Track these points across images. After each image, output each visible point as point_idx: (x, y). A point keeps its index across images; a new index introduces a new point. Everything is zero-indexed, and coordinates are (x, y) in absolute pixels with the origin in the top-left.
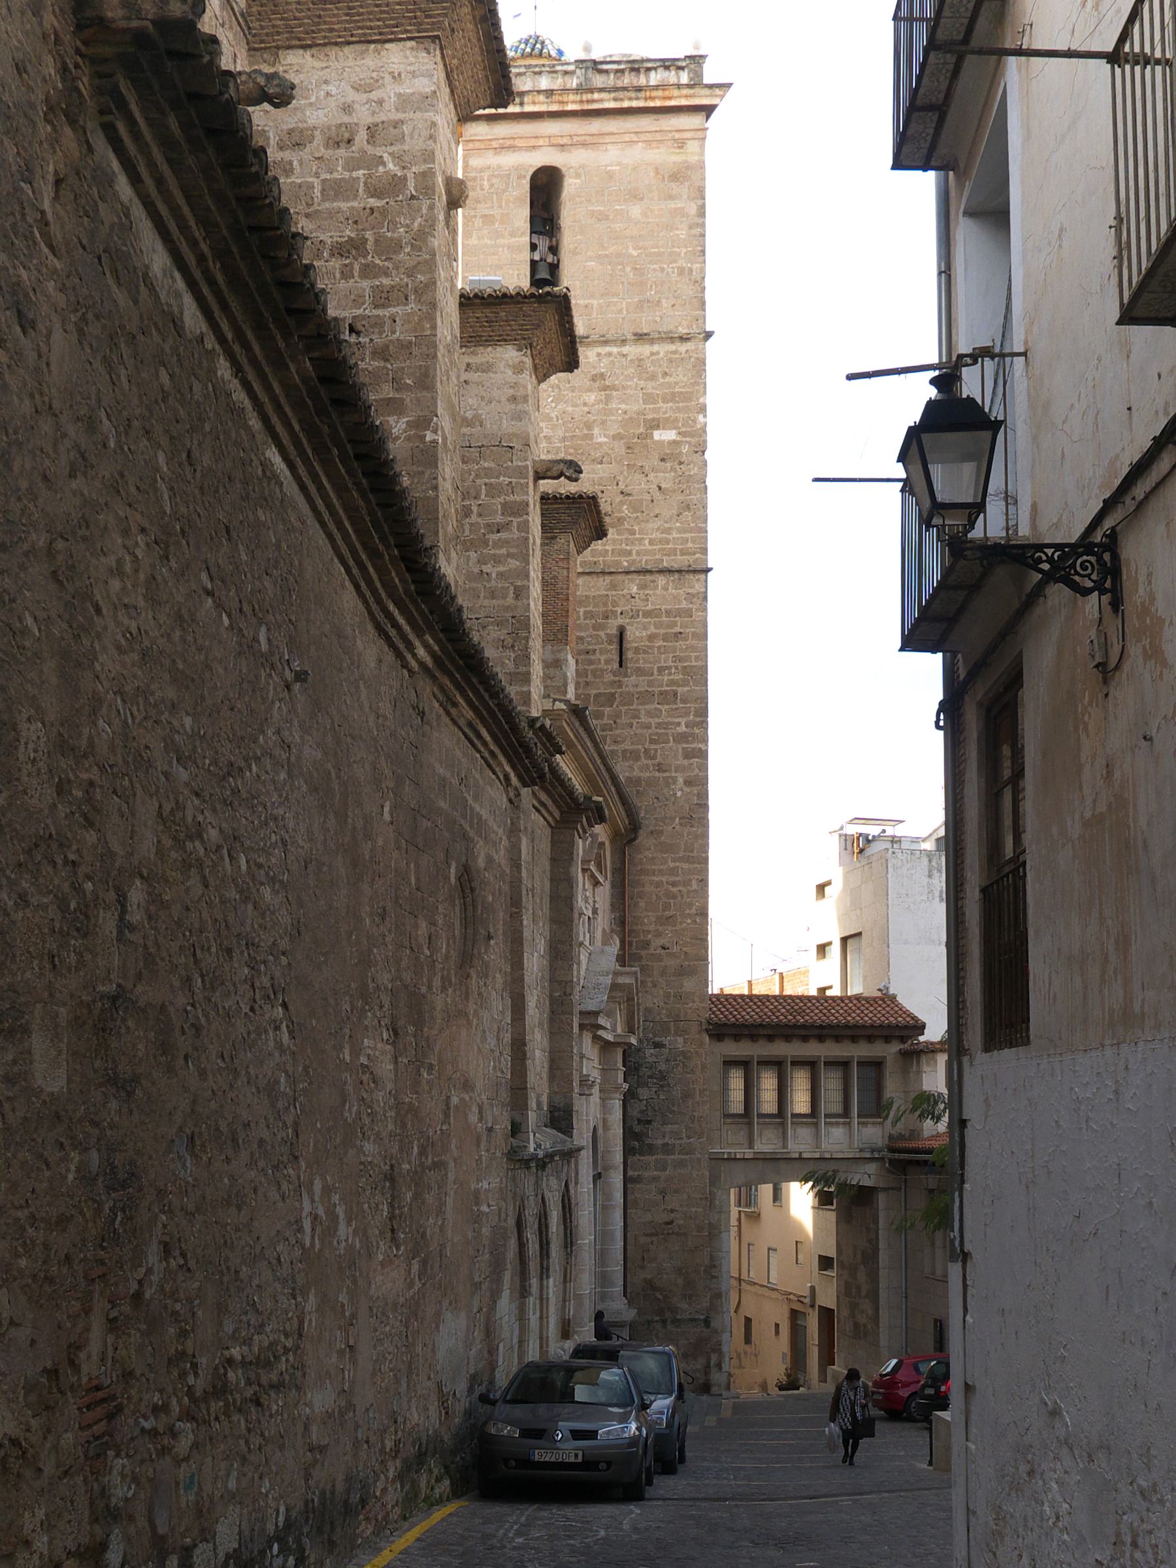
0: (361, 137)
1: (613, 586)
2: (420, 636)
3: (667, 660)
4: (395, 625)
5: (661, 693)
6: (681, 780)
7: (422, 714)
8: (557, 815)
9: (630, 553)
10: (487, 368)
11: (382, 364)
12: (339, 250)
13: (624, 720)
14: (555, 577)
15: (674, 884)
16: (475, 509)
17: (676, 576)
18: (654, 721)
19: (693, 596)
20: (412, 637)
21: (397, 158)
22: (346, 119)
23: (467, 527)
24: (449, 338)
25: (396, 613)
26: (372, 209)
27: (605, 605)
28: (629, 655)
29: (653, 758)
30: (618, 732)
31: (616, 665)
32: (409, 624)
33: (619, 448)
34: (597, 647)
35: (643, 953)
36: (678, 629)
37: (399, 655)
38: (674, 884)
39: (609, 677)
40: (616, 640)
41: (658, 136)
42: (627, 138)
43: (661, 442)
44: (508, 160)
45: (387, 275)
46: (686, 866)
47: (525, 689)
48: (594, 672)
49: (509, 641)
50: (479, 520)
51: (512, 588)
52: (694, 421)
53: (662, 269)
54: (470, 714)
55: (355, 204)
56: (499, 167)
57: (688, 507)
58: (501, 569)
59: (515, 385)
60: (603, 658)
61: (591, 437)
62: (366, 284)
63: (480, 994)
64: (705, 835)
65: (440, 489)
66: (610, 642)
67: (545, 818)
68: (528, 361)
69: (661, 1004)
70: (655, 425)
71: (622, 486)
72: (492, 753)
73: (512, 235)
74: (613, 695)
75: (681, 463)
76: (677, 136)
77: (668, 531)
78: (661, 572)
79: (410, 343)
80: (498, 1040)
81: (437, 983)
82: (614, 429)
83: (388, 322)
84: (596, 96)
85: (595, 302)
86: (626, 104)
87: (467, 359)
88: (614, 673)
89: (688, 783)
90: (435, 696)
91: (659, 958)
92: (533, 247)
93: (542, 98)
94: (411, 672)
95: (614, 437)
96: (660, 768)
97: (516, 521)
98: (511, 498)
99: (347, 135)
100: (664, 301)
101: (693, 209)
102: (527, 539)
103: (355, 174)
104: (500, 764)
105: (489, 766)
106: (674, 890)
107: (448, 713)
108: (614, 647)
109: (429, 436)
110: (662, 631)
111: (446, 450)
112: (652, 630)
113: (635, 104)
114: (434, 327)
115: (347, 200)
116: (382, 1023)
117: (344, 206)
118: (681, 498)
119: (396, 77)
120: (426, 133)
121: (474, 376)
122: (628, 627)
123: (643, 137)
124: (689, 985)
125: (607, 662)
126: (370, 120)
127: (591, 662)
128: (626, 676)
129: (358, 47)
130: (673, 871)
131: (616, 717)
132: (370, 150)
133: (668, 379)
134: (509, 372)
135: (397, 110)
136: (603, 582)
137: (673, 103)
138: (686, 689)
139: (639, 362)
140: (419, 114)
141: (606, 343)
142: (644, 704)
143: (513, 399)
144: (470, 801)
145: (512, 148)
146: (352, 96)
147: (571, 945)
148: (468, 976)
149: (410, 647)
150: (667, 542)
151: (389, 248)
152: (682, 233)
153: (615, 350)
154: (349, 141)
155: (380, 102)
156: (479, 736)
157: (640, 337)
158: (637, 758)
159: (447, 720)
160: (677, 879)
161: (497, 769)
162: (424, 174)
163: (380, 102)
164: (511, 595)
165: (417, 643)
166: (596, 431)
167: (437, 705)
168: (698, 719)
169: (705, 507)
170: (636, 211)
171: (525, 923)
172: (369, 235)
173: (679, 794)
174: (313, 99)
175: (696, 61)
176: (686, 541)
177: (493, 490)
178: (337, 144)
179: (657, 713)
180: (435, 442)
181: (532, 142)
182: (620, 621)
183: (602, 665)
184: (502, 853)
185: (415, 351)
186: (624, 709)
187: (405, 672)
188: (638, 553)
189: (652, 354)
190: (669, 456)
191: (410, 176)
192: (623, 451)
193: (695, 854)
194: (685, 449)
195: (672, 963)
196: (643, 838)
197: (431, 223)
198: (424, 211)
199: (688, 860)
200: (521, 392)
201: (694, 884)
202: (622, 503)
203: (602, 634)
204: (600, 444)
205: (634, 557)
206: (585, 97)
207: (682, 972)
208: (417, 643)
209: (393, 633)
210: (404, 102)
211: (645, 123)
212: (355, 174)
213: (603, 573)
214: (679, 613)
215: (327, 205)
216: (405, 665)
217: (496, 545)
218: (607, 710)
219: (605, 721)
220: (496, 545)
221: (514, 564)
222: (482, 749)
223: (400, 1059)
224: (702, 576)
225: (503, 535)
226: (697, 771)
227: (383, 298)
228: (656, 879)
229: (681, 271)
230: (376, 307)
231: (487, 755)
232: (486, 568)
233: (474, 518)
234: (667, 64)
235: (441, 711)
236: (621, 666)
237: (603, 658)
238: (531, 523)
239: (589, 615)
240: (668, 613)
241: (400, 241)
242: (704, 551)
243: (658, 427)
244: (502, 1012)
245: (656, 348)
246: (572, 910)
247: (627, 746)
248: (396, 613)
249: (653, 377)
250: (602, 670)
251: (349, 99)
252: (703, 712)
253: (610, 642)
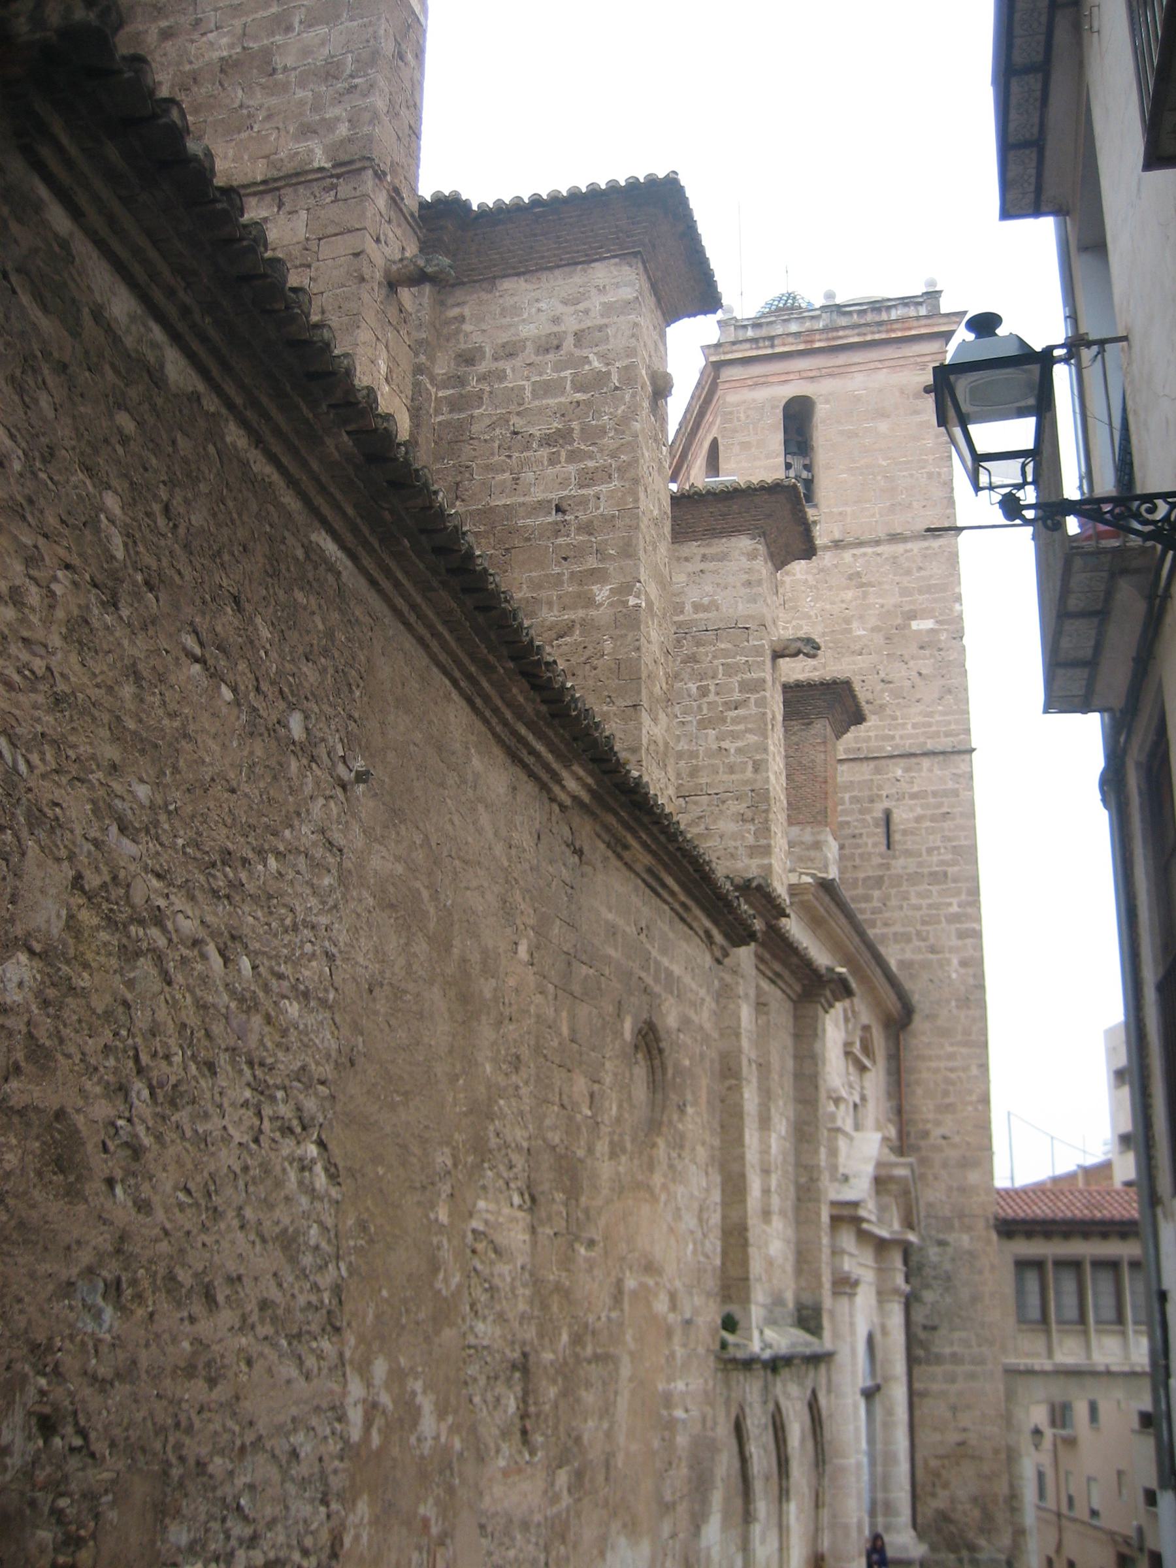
0: (569, 342)
1: (878, 771)
2: (567, 767)
3: (935, 840)
4: (532, 752)
5: (931, 874)
6: (955, 962)
7: (579, 852)
8: (798, 988)
9: (893, 738)
10: (723, 557)
11: (586, 538)
12: (548, 441)
13: (893, 902)
14: (813, 761)
15: (952, 1070)
16: (712, 688)
17: (941, 758)
18: (924, 902)
19: (959, 776)
20: (556, 766)
21: (602, 356)
22: (556, 329)
23: (705, 707)
24: (656, 512)
25: (531, 738)
26: (578, 403)
27: (870, 789)
28: (897, 837)
29: (924, 940)
30: (887, 915)
31: (883, 848)
32: (551, 751)
33: (879, 639)
34: (864, 831)
35: (922, 1143)
36: (945, 810)
37: (544, 787)
38: (952, 1070)
39: (877, 860)
40: (883, 823)
41: (901, 362)
42: (872, 366)
43: (919, 631)
44: (762, 394)
45: (591, 458)
46: (964, 1050)
47: (766, 862)
48: (861, 856)
49: (749, 814)
50: (716, 698)
51: (750, 763)
52: (951, 610)
53: (911, 476)
54: (648, 859)
55: (563, 399)
56: (754, 400)
57: (949, 691)
58: (740, 744)
59: (749, 571)
60: (870, 842)
61: (849, 631)
62: (572, 468)
63: (671, 1167)
64: (984, 1018)
65: (644, 650)
66: (877, 825)
67: (784, 991)
68: (762, 548)
69: (944, 1198)
70: (913, 615)
71: (882, 675)
72: (683, 905)
73: (768, 457)
74: (881, 878)
75: (940, 650)
76: (919, 360)
77: (930, 715)
78: (925, 754)
79: (613, 516)
80: (700, 1219)
81: (602, 1147)
82: (873, 621)
83: (593, 500)
84: (841, 333)
85: (849, 510)
86: (869, 338)
87: (703, 550)
88: (882, 856)
89: (964, 963)
90: (599, 836)
91: (939, 1149)
92: (788, 466)
93: (791, 340)
94: (563, 807)
95: (875, 629)
96: (933, 950)
97: (753, 697)
98: (748, 676)
99: (555, 342)
100: (915, 504)
102: (764, 714)
103: (562, 374)
104: (696, 918)
105: (683, 919)
106: (953, 1076)
107: (620, 857)
108: (881, 830)
109: (632, 601)
110: (929, 812)
111: (653, 615)
112: (919, 811)
113: (877, 337)
114: (637, 500)
115: (555, 396)
116: (512, 1185)
117: (552, 402)
118: (942, 682)
119: (602, 290)
120: (628, 333)
121: (709, 566)
122: (895, 811)
123: (887, 364)
124: (973, 1177)
125: (875, 845)
126: (576, 327)
127: (858, 846)
128: (894, 857)
129: (566, 269)
130: (951, 1056)
131: (884, 901)
132: (578, 353)
133: (923, 573)
134: (744, 559)
135: (602, 316)
136: (866, 770)
137: (913, 332)
138: (956, 869)
139: (894, 560)
140: (622, 318)
141: (861, 544)
142: (914, 885)
143: (749, 583)
144: (655, 953)
146: (561, 309)
147: (817, 1127)
148: (654, 1145)
149: (559, 781)
150: (930, 725)
151: (593, 435)
153: (869, 550)
154: (558, 347)
155: (586, 312)
156: (664, 886)
157: (894, 538)
158: (909, 940)
159: (619, 864)
160: (956, 1064)
161: (695, 925)
162: (626, 368)
163: (586, 312)
164: (750, 768)
165: (565, 774)
166: (855, 625)
167: (602, 846)
168: (971, 899)
169: (966, 690)
170: (883, 426)
171: (746, 1095)
172: (575, 425)
173: (954, 976)
174: (525, 316)
175: (933, 296)
176: (949, 723)
177: (730, 670)
178: (547, 351)
179: (927, 894)
180: (638, 606)
181: (783, 378)
182: (886, 804)
183: (870, 849)
184: (705, 1014)
185: (618, 523)
186: (893, 891)
187: (556, 807)
188: (901, 737)
189: (906, 551)
190: (927, 643)
191: (614, 370)
192: (882, 641)
193: (973, 1037)
194: (943, 636)
195: (953, 1154)
196: (918, 1023)
197: (633, 410)
198: (627, 397)
199: (966, 1044)
200: (755, 577)
201: (974, 1071)
202: (883, 691)
203: (868, 817)
204: (859, 637)
205: (898, 740)
206: (830, 335)
207: (966, 1163)
208: (565, 774)
209: (530, 760)
210: (608, 309)
211: (889, 352)
212: (562, 374)
213: (867, 759)
214: (946, 793)
215: (537, 403)
216: (553, 800)
217: (735, 721)
218: (876, 893)
219: (876, 904)
220: (735, 721)
221: (752, 738)
222: (670, 899)
223: (540, 1230)
224: (966, 757)
225: (741, 712)
226: (971, 952)
227: (588, 479)
228: (933, 1064)
229: (930, 476)
230: (581, 487)
231: (677, 906)
232: (724, 745)
233: (712, 697)
234: (905, 302)
235: (610, 853)
236: (889, 847)
237: (870, 842)
238: (769, 699)
239: (855, 800)
240: (935, 794)
241: (604, 427)
242: (967, 731)
243: (915, 618)
244: (707, 1190)
245: (909, 546)
246: (816, 1087)
247: (898, 928)
248: (531, 738)
249: (908, 572)
250: (870, 854)
251: (558, 313)
252: (975, 892)
253: (877, 825)
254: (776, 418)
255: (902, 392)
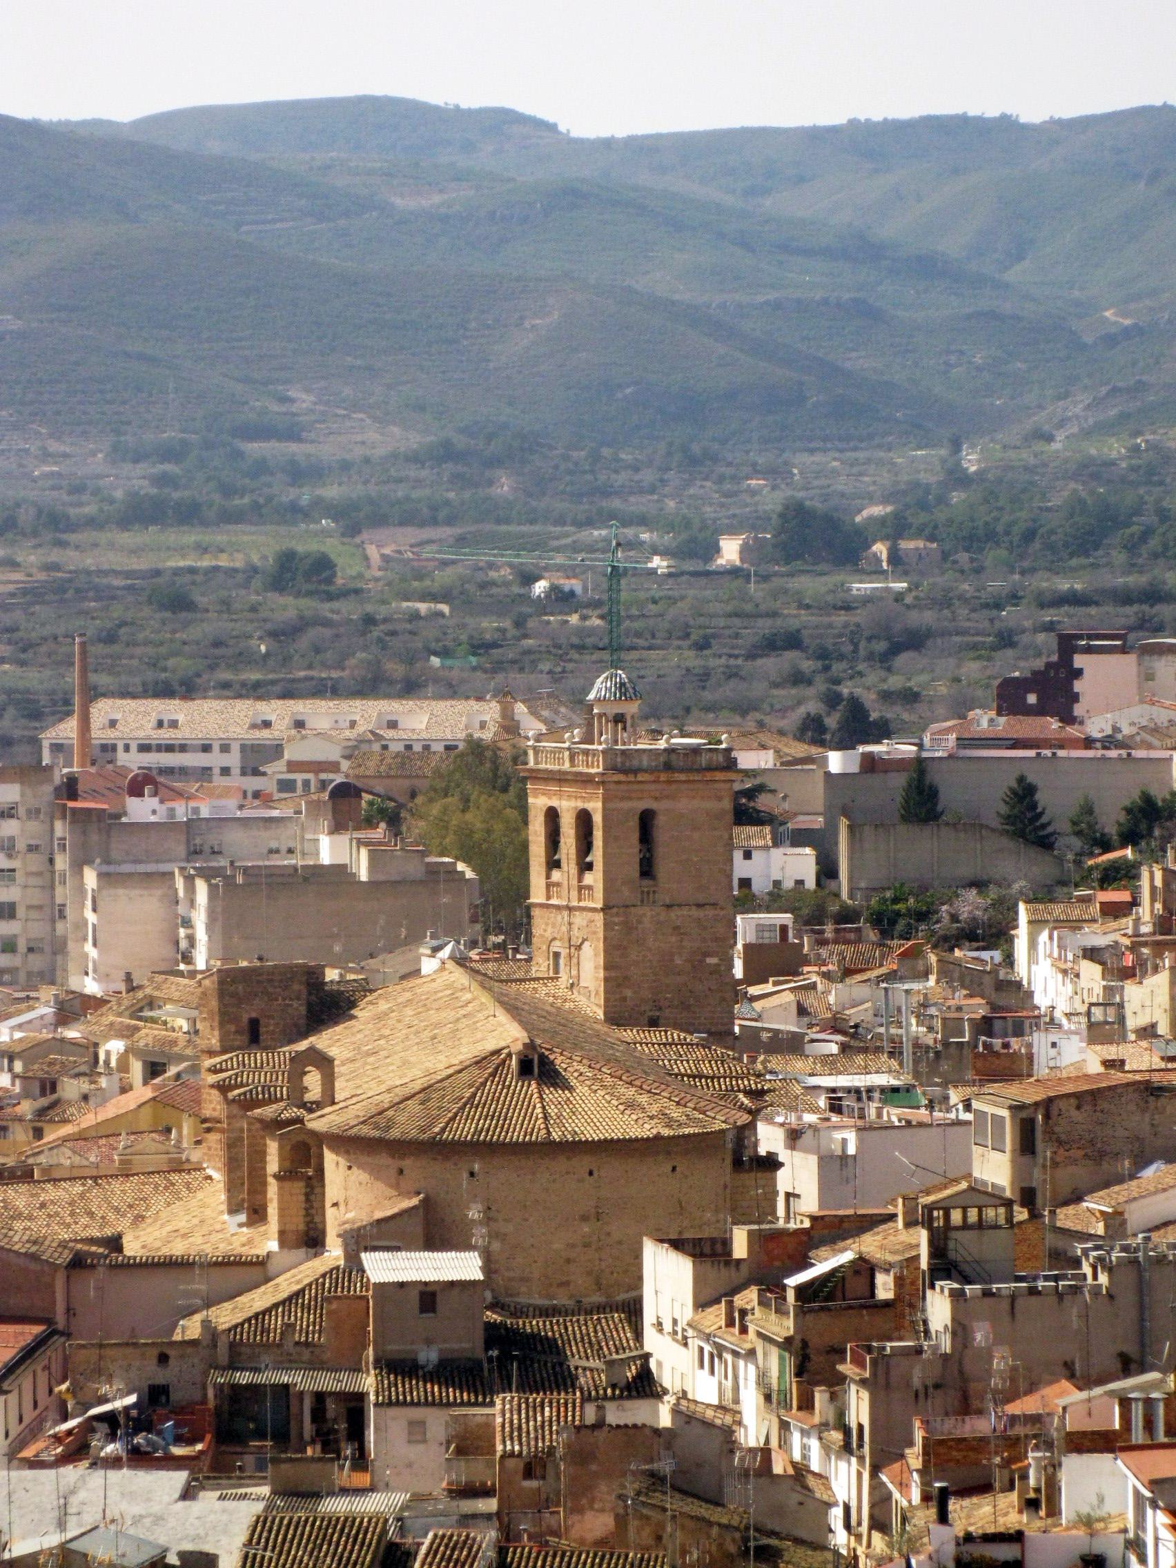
44: (626, 805)
61: (672, 960)
101: (726, 836)
145: (630, 799)
152: (721, 850)
170: (696, 835)
211: (700, 786)
249: (705, 928)
254: (634, 823)
255: (708, 814)
